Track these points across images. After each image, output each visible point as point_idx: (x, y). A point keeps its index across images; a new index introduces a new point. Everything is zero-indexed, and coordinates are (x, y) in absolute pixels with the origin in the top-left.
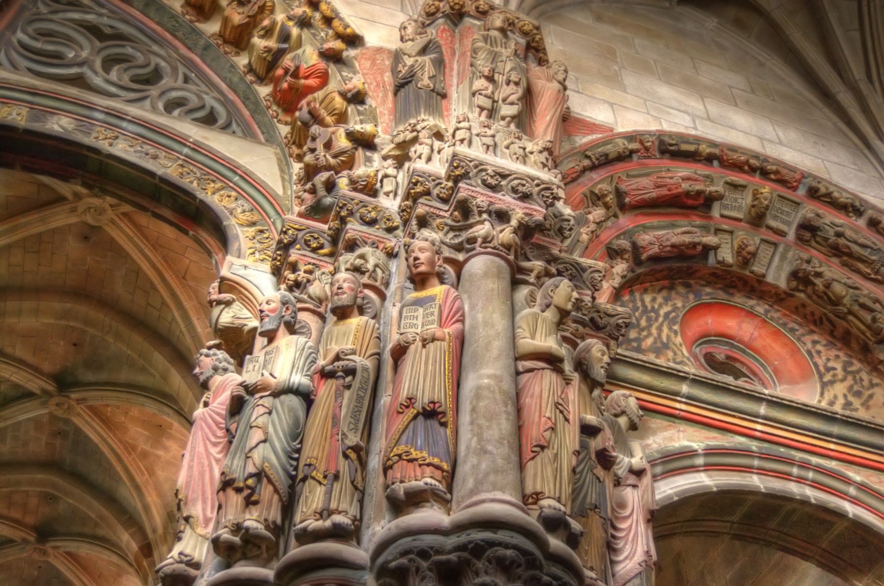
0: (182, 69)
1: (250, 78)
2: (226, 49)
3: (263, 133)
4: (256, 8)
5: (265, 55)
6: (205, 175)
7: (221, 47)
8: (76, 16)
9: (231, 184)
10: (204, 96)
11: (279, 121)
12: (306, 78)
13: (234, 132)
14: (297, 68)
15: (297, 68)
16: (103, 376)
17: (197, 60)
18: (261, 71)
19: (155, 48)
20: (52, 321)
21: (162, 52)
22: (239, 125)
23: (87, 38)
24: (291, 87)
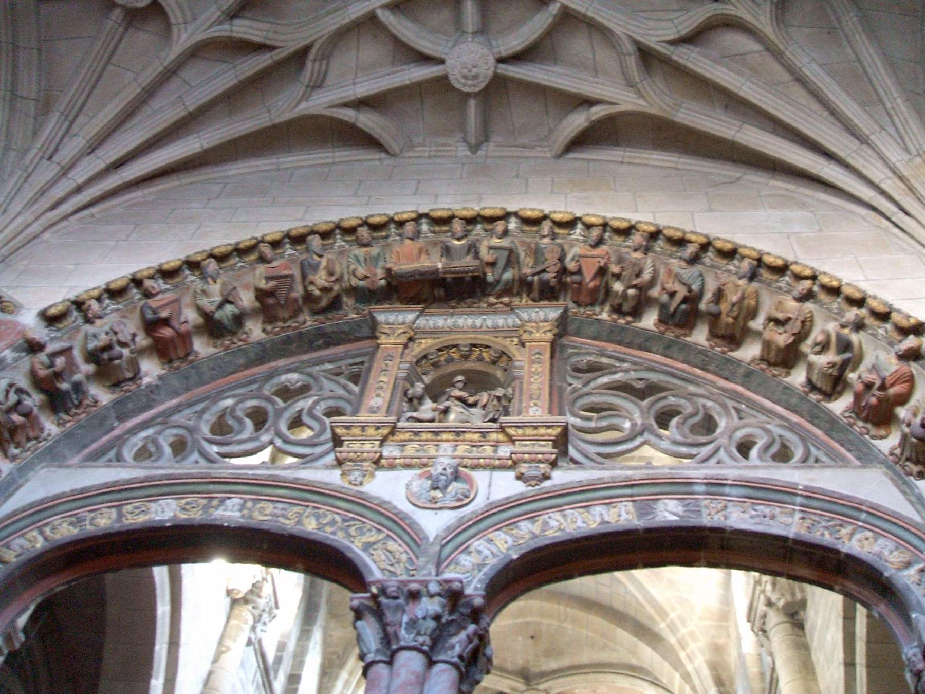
0: (730, 403)
1: (814, 397)
2: (774, 372)
3: (849, 451)
4: (798, 324)
5: (831, 370)
6: (829, 521)
7: (767, 371)
8: (605, 380)
9: (860, 524)
10: (769, 426)
11: (873, 437)
12: (892, 385)
13: (817, 461)
14: (884, 380)
15: (884, 380)
16: (566, 662)
17: (740, 389)
18: (827, 388)
19: (692, 388)
20: (511, 622)
21: (701, 391)
22: (819, 449)
23: (632, 401)
24: (880, 400)
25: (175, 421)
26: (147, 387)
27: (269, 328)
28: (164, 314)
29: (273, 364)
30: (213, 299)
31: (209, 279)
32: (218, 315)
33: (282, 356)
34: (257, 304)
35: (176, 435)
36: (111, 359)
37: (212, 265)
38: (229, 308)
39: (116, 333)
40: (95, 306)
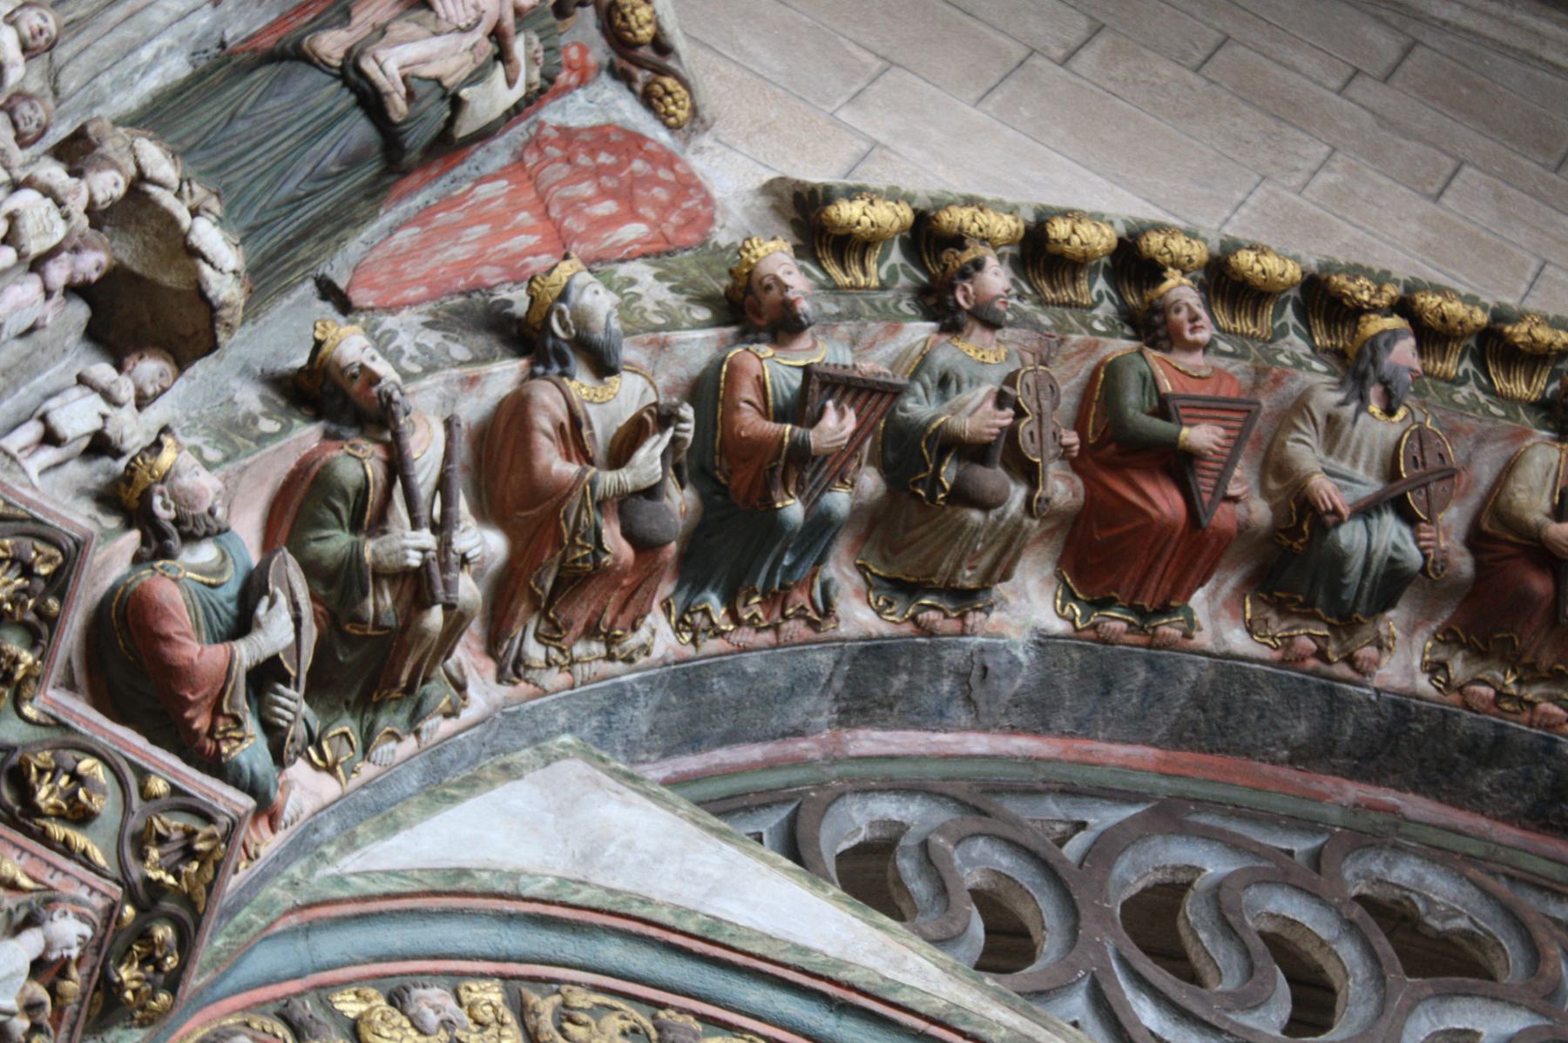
25: (1015, 823)
26: (982, 650)
27: (1458, 668)
28: (1201, 435)
29: (1389, 797)
30: (1345, 467)
31: (1374, 392)
32: (1351, 536)
33: (1426, 785)
34: (1464, 564)
35: (998, 874)
36: (963, 496)
37: (1404, 353)
38: (1390, 532)
39: (1020, 413)
40: (996, 278)
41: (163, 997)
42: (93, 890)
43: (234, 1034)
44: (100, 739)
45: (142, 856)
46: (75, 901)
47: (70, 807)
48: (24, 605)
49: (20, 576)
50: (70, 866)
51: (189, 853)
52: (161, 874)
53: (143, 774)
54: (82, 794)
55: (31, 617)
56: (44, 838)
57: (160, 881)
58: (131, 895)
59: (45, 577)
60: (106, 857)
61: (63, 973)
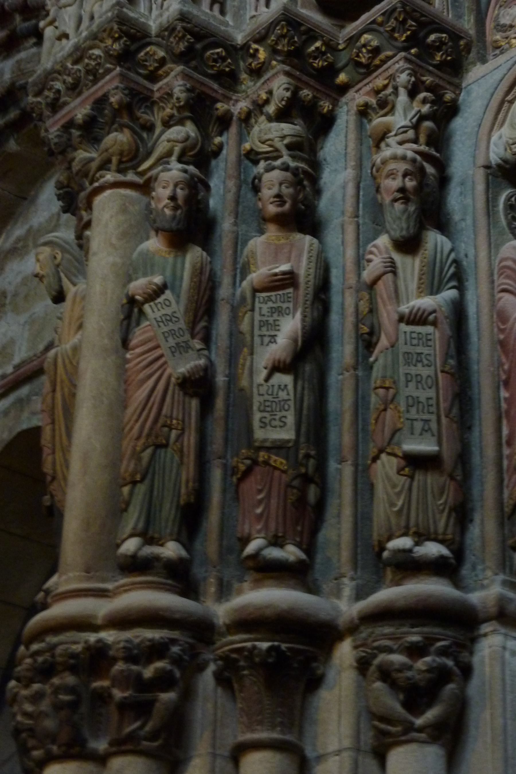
41: (462, 43)
42: (397, 62)
43: (498, 15)
44: (360, 28)
45: (396, 39)
46: (397, 71)
47: (371, 53)
48: (295, 42)
49: (285, 40)
50: (389, 63)
51: (404, 22)
52: (405, 35)
53: (374, 22)
54: (369, 48)
55: (304, 37)
56: (378, 67)
57: (407, 37)
58: (406, 49)
59: (288, 31)
60: (391, 50)
61: (423, 82)
